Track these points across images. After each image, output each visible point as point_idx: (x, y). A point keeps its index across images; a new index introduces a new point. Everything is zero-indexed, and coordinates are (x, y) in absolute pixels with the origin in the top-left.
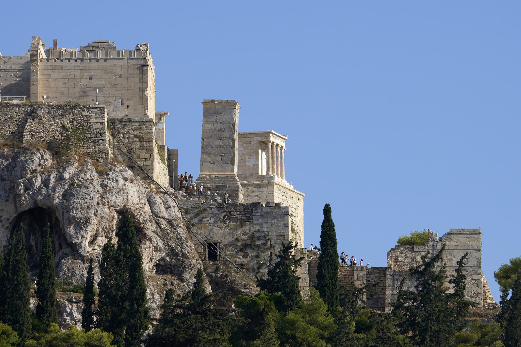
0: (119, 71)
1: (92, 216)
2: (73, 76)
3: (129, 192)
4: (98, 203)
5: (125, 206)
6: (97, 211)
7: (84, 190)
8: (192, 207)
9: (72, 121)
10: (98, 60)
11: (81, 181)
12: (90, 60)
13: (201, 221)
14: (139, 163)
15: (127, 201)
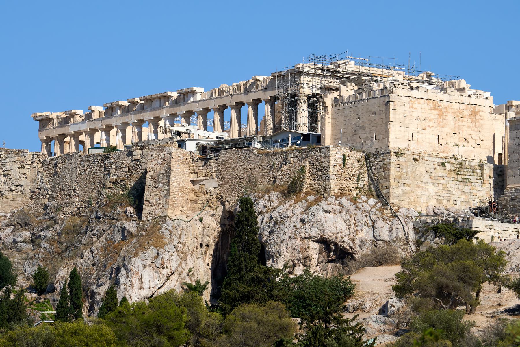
0: (374, 110)
1: (283, 249)
2: (349, 118)
3: (325, 224)
4: (290, 237)
5: (321, 236)
6: (287, 245)
7: (282, 227)
8: (421, 227)
9: (311, 162)
10: (363, 101)
11: (283, 219)
12: (359, 101)
13: (426, 239)
14: (382, 192)
15: (324, 232)
